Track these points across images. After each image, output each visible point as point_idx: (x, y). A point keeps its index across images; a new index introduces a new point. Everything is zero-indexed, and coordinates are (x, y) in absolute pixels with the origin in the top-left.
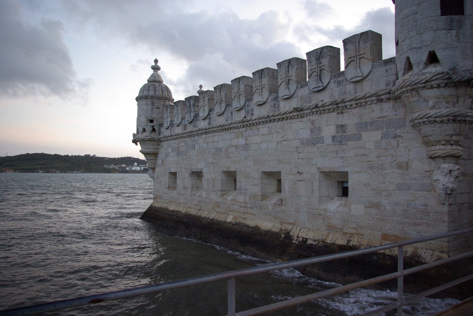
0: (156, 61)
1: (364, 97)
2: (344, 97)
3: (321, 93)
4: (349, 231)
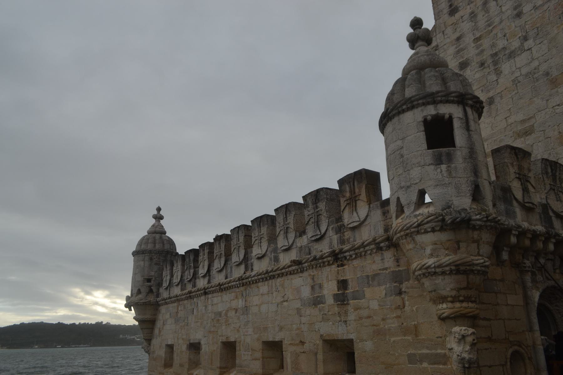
0: (159, 209)
1: (363, 246)
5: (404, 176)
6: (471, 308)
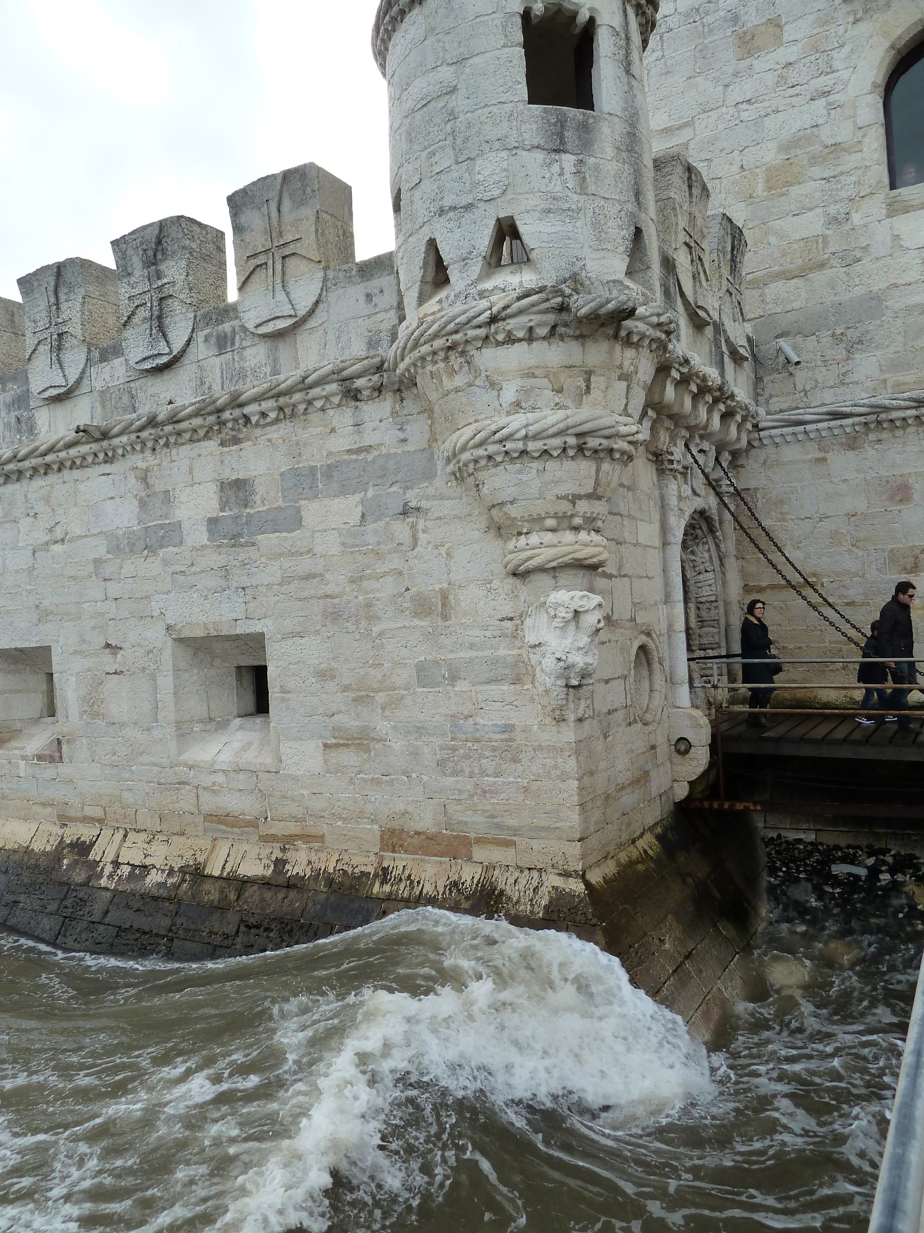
1: (304, 385)
2: (239, 387)
3: (167, 375)
4: (279, 829)
5: (455, 175)
6: (595, 546)
